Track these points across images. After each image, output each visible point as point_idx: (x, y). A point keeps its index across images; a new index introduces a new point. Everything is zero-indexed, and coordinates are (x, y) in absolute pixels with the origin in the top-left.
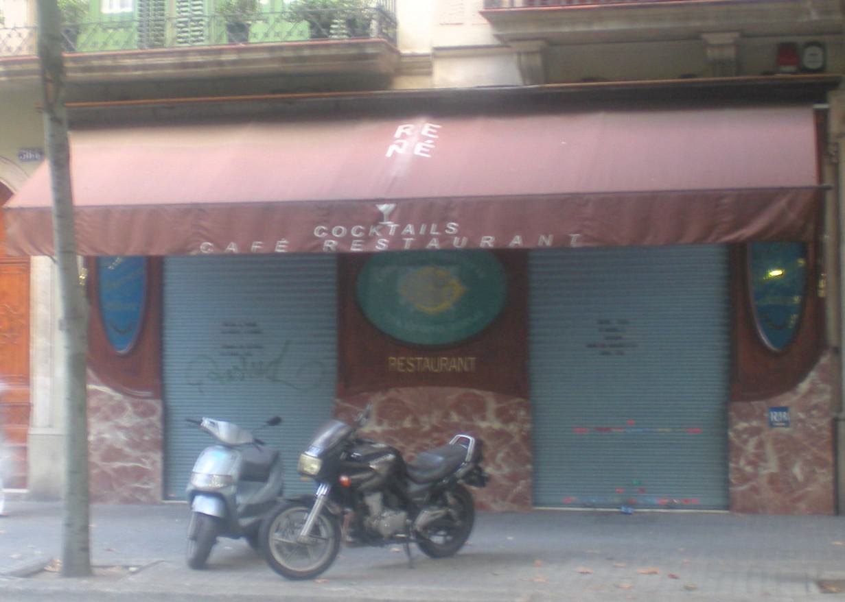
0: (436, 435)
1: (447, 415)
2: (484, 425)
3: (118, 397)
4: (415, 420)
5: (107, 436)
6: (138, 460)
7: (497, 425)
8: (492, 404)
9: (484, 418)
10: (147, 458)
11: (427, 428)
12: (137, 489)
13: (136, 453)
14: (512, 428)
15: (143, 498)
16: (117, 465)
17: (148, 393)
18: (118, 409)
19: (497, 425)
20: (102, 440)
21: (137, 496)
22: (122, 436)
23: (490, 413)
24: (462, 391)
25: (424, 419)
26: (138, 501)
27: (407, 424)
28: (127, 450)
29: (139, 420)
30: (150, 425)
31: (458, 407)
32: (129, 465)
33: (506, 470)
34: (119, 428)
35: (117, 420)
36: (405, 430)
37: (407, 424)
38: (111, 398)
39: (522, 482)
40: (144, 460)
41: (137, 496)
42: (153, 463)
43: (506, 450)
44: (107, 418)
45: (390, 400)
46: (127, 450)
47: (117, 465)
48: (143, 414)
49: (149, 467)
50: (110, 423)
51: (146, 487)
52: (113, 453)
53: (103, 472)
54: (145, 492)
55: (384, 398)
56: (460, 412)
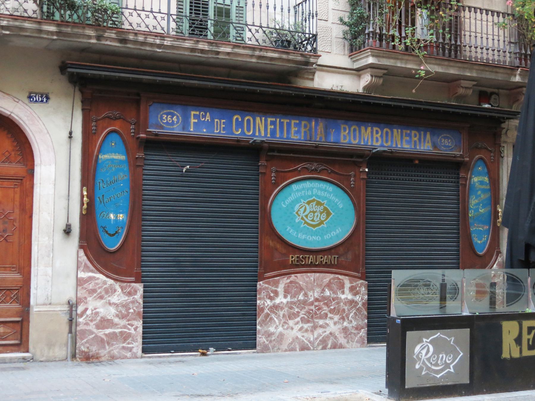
0: (316, 304)
1: (323, 291)
2: (343, 297)
3: (110, 282)
4: (306, 295)
8: (348, 285)
9: (343, 293)
11: (312, 299)
13: (123, 322)
14: (357, 298)
17: (133, 279)
18: (110, 291)
19: (350, 297)
22: (113, 310)
23: (347, 290)
24: (332, 276)
25: (310, 293)
28: (116, 320)
29: (127, 298)
33: (354, 323)
35: (110, 298)
36: (299, 301)
37: (301, 297)
38: (105, 283)
39: (363, 330)
40: (129, 327)
42: (135, 329)
43: (355, 311)
44: (101, 298)
45: (291, 282)
46: (116, 320)
48: (129, 294)
51: (129, 346)
52: (105, 323)
54: (130, 350)
55: (288, 281)
56: (330, 289)
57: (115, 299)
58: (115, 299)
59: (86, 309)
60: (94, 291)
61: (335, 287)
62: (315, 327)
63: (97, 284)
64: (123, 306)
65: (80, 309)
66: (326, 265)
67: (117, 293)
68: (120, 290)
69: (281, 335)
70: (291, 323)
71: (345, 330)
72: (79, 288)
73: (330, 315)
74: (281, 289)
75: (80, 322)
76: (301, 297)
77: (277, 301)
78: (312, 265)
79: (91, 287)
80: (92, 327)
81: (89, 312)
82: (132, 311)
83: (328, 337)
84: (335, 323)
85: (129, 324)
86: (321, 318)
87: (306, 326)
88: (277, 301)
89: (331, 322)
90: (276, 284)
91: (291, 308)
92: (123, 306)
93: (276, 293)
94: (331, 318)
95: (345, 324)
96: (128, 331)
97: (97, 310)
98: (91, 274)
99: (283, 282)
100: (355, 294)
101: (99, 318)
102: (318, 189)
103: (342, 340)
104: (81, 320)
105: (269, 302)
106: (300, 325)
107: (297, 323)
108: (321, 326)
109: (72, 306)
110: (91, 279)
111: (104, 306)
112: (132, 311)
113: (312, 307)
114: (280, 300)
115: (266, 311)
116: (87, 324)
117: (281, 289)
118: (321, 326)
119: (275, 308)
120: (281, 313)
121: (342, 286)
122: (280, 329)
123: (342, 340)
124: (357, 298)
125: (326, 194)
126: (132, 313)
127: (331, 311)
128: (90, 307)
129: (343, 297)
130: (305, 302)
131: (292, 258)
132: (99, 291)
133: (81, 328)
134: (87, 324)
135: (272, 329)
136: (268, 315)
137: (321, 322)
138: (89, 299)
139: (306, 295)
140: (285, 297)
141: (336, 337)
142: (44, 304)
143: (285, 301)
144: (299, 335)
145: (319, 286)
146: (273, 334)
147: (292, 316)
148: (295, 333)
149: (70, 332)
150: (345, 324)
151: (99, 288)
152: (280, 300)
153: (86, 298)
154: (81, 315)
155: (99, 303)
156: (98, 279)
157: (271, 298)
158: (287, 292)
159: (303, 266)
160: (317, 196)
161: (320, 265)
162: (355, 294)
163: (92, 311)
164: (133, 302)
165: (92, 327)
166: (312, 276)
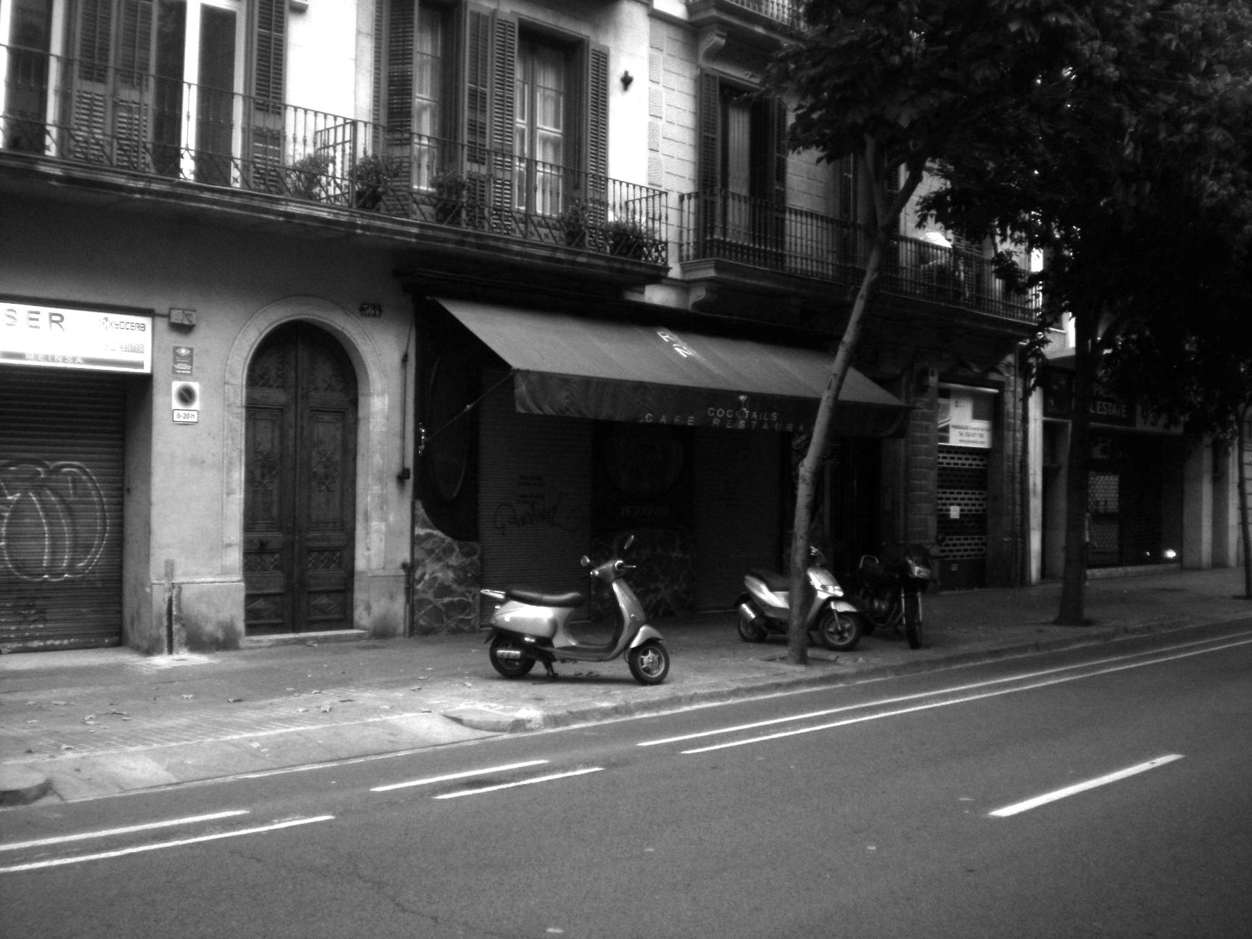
2: (674, 555)
3: (448, 540)
5: (439, 574)
6: (463, 594)
7: (680, 555)
10: (470, 592)
12: (462, 621)
13: (461, 589)
15: (466, 628)
16: (447, 600)
18: (448, 551)
19: (680, 555)
20: (435, 579)
21: (462, 626)
22: (451, 574)
26: (462, 631)
28: (454, 586)
29: (464, 560)
30: (471, 564)
32: (456, 599)
34: (448, 567)
38: (443, 541)
41: (462, 626)
44: (439, 559)
46: (454, 586)
47: (447, 600)
48: (467, 555)
49: (470, 600)
50: (442, 563)
51: (467, 618)
52: (443, 590)
53: (435, 607)
58: (453, 560)
59: (424, 574)
63: (435, 542)
65: (418, 574)
67: (455, 554)
68: (458, 550)
72: (416, 548)
75: (418, 590)
80: (430, 596)
81: (427, 577)
82: (469, 575)
84: (666, 587)
85: (467, 591)
89: (661, 585)
95: (676, 587)
96: (465, 599)
97: (436, 575)
98: (429, 531)
101: (436, 585)
104: (419, 587)
110: (429, 536)
111: (441, 570)
112: (469, 575)
126: (470, 578)
128: (429, 571)
132: (437, 551)
133: (420, 597)
138: (427, 561)
150: (676, 587)
151: (438, 547)
153: (423, 560)
154: (419, 582)
155: (437, 566)
156: (436, 536)
163: (430, 575)
165: (430, 596)
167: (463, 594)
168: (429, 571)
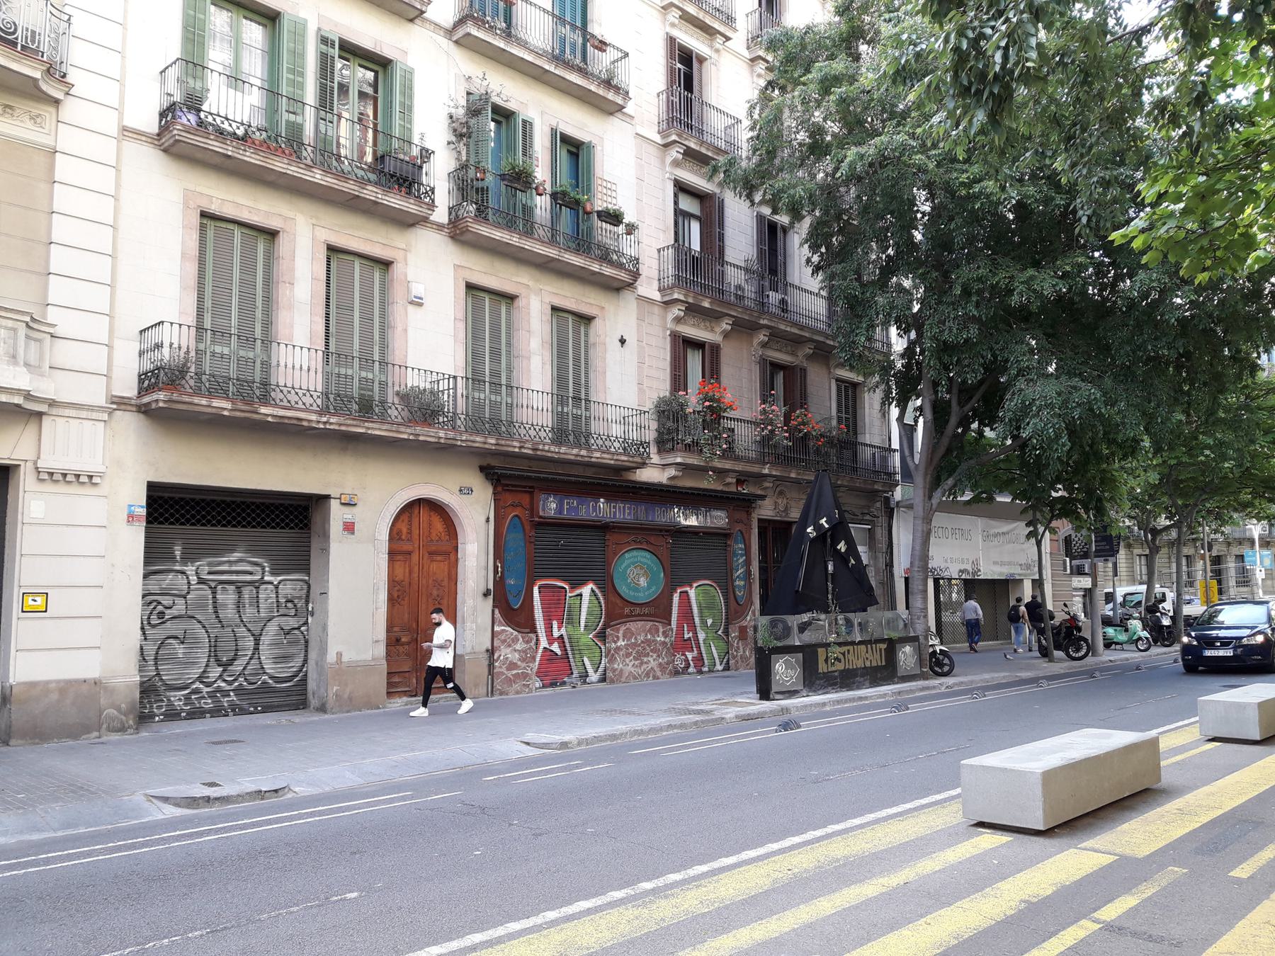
2: (658, 639)
4: (636, 639)
5: (510, 656)
6: (525, 668)
9: (658, 636)
11: (640, 642)
13: (524, 665)
14: (667, 640)
16: (514, 672)
17: (528, 630)
18: (515, 640)
19: (663, 639)
23: (660, 634)
24: (652, 623)
27: (633, 641)
28: (519, 663)
31: (649, 631)
38: (512, 634)
44: (510, 646)
46: (519, 663)
47: (514, 672)
48: (527, 642)
49: (530, 672)
52: (512, 666)
57: (518, 647)
58: (518, 647)
60: (504, 641)
61: (653, 631)
62: (642, 664)
64: (524, 652)
65: (496, 656)
66: (647, 615)
69: (621, 670)
70: (627, 660)
71: (660, 664)
72: (495, 639)
73: (651, 654)
74: (620, 635)
76: (633, 641)
77: (619, 644)
78: (639, 615)
79: (503, 638)
80: (504, 670)
81: (502, 658)
83: (650, 671)
86: (645, 656)
87: (636, 663)
88: (619, 644)
90: (618, 631)
91: (627, 649)
92: (524, 652)
93: (618, 639)
94: (652, 656)
98: (503, 628)
99: (623, 629)
100: (666, 637)
102: (641, 557)
103: (659, 673)
104: (497, 664)
105: (613, 645)
106: (632, 663)
107: (631, 661)
108: (646, 663)
109: (491, 652)
111: (511, 652)
113: (640, 648)
114: (621, 643)
115: (612, 652)
116: (500, 667)
117: (620, 635)
118: (646, 663)
119: (618, 649)
120: (621, 653)
121: (657, 631)
122: (621, 665)
123: (659, 673)
124: (667, 640)
125: (646, 561)
127: (652, 651)
128: (503, 654)
129: (658, 639)
130: (635, 645)
131: (627, 611)
134: (500, 667)
135: (616, 666)
136: (613, 655)
137: (645, 659)
139: (636, 639)
140: (624, 641)
141: (655, 671)
142: (471, 653)
143: (623, 643)
144: (632, 670)
145: (644, 631)
146: (616, 669)
147: (628, 655)
148: (630, 668)
149: (489, 674)
152: (621, 643)
154: (497, 661)
155: (508, 650)
157: (615, 642)
158: (624, 637)
159: (635, 616)
160: (641, 562)
161: (644, 615)
162: (666, 637)
164: (529, 649)
166: (640, 624)
167: (525, 668)
168: (503, 654)
